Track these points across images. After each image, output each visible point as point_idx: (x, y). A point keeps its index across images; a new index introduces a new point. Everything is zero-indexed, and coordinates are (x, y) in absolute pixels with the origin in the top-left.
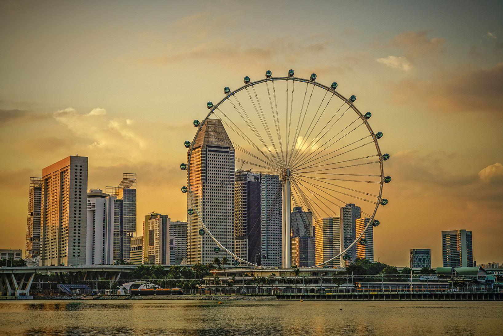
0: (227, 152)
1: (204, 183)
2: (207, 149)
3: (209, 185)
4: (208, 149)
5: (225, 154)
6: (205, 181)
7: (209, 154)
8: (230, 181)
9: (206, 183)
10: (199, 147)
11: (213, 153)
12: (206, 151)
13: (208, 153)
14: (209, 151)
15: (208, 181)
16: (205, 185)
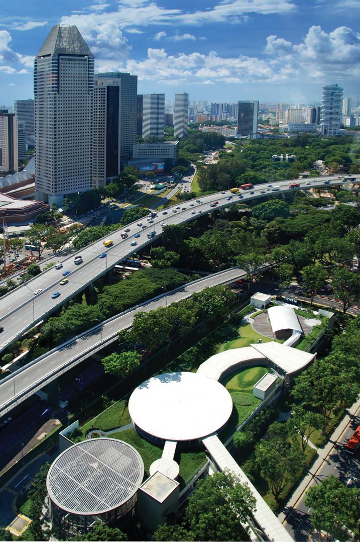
0: (85, 60)
1: (55, 94)
2: (59, 57)
3: (63, 96)
4: (61, 57)
5: (83, 62)
6: (56, 92)
7: (61, 63)
8: (89, 90)
9: (59, 94)
10: (49, 55)
11: (68, 62)
12: (58, 60)
13: (61, 61)
14: (62, 59)
15: (61, 92)
16: (57, 96)
